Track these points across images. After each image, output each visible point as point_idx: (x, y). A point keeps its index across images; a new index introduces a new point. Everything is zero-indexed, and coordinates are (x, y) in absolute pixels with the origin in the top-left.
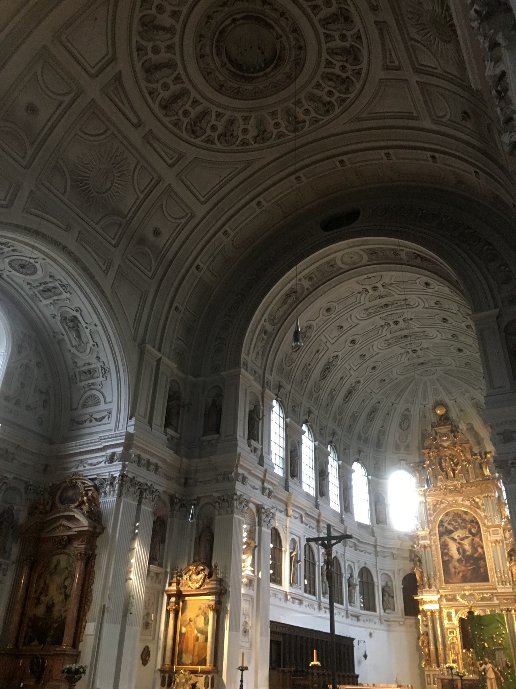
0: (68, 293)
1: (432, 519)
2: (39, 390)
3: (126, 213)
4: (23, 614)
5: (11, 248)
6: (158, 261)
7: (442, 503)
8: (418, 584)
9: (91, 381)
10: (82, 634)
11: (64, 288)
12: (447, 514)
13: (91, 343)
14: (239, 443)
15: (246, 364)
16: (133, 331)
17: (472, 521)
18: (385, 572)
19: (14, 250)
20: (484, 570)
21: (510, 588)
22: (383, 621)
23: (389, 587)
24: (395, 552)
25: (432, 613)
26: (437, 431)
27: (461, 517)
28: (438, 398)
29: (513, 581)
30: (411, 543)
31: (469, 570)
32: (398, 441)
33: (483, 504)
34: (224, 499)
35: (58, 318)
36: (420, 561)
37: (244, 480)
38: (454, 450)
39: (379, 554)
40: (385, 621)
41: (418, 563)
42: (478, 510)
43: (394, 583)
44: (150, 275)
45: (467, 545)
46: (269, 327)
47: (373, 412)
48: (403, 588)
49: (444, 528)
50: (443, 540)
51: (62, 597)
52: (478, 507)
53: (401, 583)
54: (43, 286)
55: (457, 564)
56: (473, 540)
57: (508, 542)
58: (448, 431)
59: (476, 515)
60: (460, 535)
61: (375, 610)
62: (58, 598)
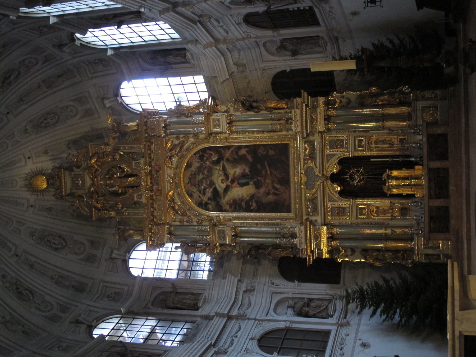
1: (196, 219)
7: (173, 200)
8: (292, 256)
12: (191, 196)
17: (201, 158)
18: (272, 307)
20: (271, 149)
21: (295, 112)
22: (345, 320)
23: (295, 303)
24: (243, 287)
25: (331, 238)
26: (68, 192)
27: (195, 174)
28: (21, 183)
29: (287, 108)
30: (234, 258)
31: (271, 172)
32: (81, 257)
33: (178, 138)
36: (258, 247)
38: (97, 170)
39: (242, 313)
40: (345, 317)
41: (260, 251)
42: (185, 147)
43: (290, 295)
45: (235, 170)
47: (17, 289)
48: (299, 281)
49: (209, 202)
50: (227, 207)
52: (182, 145)
53: (291, 284)
55: (262, 190)
56: (228, 160)
57: (232, 109)
58: (70, 175)
59: (191, 149)
60: (221, 178)
61: (328, 333)
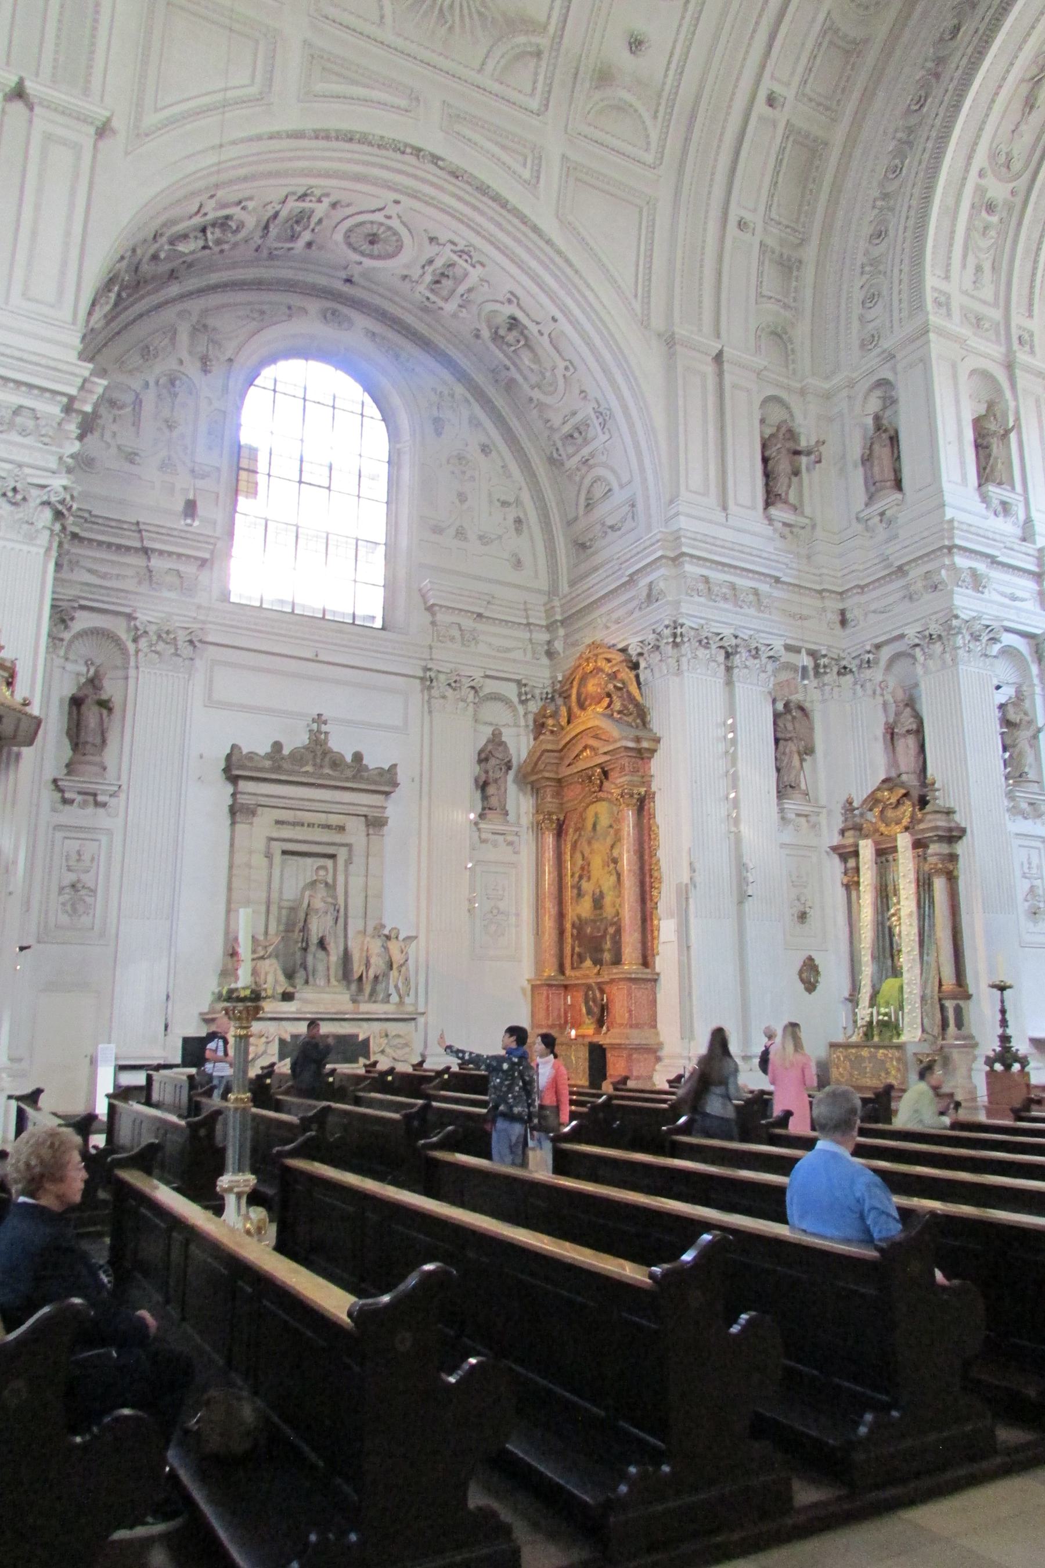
0: (478, 266)
2: (498, 500)
3: (543, 19)
4: (561, 916)
5: (326, 201)
6: (661, 114)
9: (585, 452)
10: (656, 942)
11: (465, 257)
13: (561, 364)
14: (948, 498)
15: (944, 304)
16: (637, 306)
19: (334, 205)
34: (931, 635)
35: (486, 334)
37: (977, 582)
44: (649, 158)
46: (998, 190)
51: (613, 879)
54: (429, 269)
62: (608, 882)
